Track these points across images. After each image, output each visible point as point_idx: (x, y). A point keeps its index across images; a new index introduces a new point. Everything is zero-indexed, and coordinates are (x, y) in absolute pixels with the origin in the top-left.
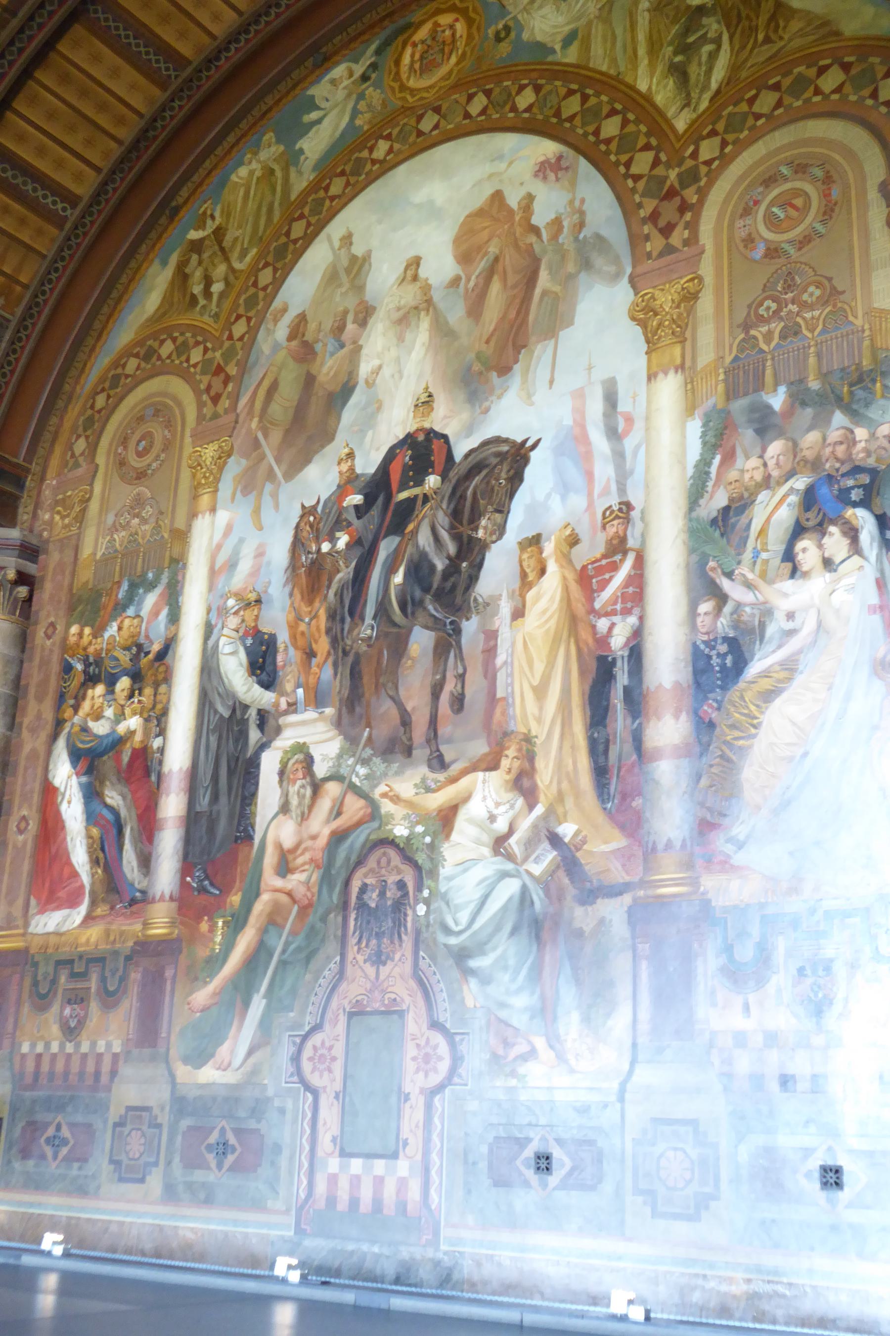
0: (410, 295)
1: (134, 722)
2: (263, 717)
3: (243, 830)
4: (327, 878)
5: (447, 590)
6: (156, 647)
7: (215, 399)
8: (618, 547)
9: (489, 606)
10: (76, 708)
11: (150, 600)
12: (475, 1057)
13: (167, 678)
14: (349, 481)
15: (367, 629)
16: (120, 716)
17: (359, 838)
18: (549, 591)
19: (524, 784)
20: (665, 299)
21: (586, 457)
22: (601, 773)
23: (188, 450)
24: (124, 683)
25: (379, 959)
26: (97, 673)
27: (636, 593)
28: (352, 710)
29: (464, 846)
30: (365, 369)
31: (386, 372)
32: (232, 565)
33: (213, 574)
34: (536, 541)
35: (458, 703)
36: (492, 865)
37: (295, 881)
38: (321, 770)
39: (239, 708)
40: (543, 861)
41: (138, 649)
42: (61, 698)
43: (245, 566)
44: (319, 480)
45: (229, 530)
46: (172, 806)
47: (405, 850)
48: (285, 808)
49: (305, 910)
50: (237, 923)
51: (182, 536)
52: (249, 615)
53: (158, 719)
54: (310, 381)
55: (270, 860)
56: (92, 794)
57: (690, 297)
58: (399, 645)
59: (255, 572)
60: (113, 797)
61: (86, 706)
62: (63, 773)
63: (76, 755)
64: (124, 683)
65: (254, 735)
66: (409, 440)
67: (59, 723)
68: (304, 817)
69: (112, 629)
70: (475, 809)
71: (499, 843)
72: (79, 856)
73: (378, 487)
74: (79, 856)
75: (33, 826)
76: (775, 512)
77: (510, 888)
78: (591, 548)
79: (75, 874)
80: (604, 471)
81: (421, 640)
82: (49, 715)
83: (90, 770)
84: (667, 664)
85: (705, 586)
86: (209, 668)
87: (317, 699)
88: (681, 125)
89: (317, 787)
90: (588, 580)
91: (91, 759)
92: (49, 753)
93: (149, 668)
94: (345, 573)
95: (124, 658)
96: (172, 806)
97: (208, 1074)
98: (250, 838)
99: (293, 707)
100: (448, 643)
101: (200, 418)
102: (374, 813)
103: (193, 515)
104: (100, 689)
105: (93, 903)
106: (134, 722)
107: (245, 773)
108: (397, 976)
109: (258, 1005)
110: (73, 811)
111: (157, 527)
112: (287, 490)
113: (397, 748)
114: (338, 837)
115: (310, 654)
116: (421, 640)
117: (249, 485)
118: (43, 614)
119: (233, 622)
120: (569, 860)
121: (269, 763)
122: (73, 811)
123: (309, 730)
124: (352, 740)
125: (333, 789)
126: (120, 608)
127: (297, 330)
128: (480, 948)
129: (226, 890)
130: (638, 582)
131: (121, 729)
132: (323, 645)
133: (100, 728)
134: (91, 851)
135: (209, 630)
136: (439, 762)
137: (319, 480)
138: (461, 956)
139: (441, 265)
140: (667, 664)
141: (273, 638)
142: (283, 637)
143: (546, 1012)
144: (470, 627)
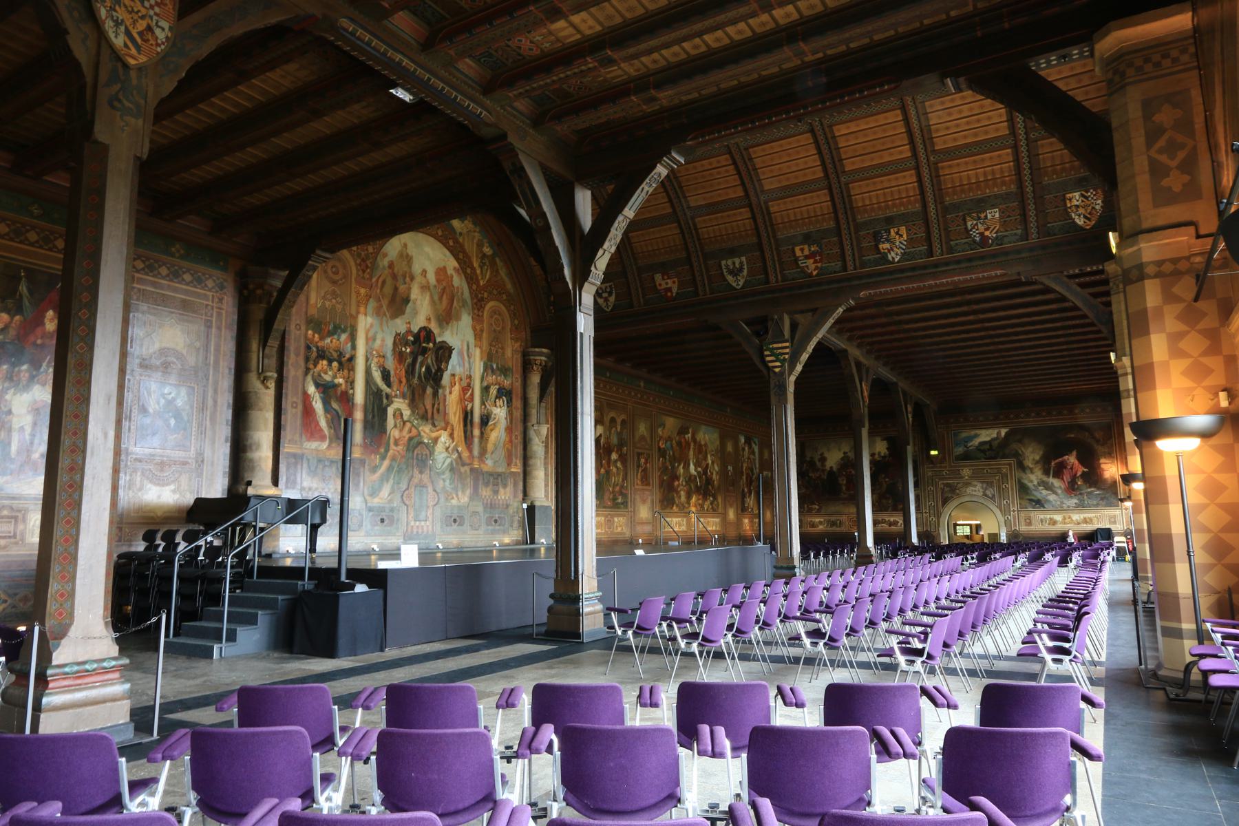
0: (424, 281)
1: (341, 381)
2: (388, 396)
3: (382, 429)
4: (408, 449)
5: (435, 378)
6: (348, 356)
7: (364, 272)
8: (469, 385)
9: (444, 388)
10: (315, 366)
11: (344, 337)
12: (442, 500)
13: (352, 369)
14: (409, 332)
15: (416, 381)
16: (335, 377)
17: (415, 440)
18: (457, 389)
19: (451, 435)
20: (478, 328)
21: (463, 359)
22: (465, 437)
23: (354, 285)
24: (335, 364)
25: (421, 472)
26: (322, 354)
27: (472, 399)
28: (413, 404)
29: (439, 448)
30: (413, 296)
31: (418, 302)
32: (374, 339)
33: (367, 339)
34: (453, 375)
35: (438, 411)
36: (445, 455)
37: (400, 448)
38: (405, 418)
39: (379, 391)
40: (455, 456)
41: (341, 355)
42: (307, 359)
43: (378, 342)
44: (400, 325)
45: (372, 325)
46: (359, 415)
47: (427, 445)
48: (395, 426)
49: (403, 457)
50: (383, 458)
51: (355, 318)
52: (382, 360)
53: (351, 383)
54: (396, 289)
55: (392, 441)
56: (326, 403)
57: (482, 331)
58: (424, 391)
59: (382, 346)
60: (335, 405)
61: (319, 367)
62: (311, 389)
63: (317, 385)
64: (335, 364)
65: (385, 401)
66: (425, 328)
67: (307, 370)
68: (401, 431)
69: (328, 340)
70: (442, 439)
71: (447, 449)
72: (323, 423)
73: (417, 336)
74: (323, 423)
75: (300, 407)
76: (493, 391)
77: (449, 461)
78: (464, 384)
79: (321, 430)
80: (467, 365)
81: (429, 391)
82: (302, 363)
83: (323, 392)
84: (477, 419)
85: (483, 403)
86: (368, 372)
87: (404, 397)
88: (482, 283)
89: (404, 423)
90: (464, 390)
91: (326, 389)
92: (304, 380)
93: (347, 363)
94: (409, 360)
95: (335, 355)
96: (359, 415)
97: (376, 500)
98: (385, 432)
99: (396, 396)
100: (435, 394)
101: (358, 275)
102: (419, 435)
103: (358, 313)
104: (325, 362)
105: (331, 442)
106: (341, 381)
107: (383, 412)
108: (425, 477)
109: (391, 481)
110: (318, 406)
111: (344, 309)
112: (391, 322)
113: (424, 417)
114: (411, 439)
115: (401, 382)
116: (429, 391)
117: (378, 312)
118: (294, 318)
119: (376, 360)
120: (460, 456)
121: (390, 411)
122: (318, 406)
123: (399, 405)
124: (413, 412)
125: (408, 425)
126: (330, 334)
127: (391, 265)
128: (443, 473)
129: (379, 447)
130: (472, 395)
131: (336, 381)
132: (404, 380)
133: (328, 378)
134: (327, 422)
135: (367, 360)
136: (434, 425)
137: (400, 325)
138: (438, 474)
139: (432, 278)
140: (477, 419)
141: (389, 372)
142: (392, 373)
143: (456, 489)
144: (440, 391)
